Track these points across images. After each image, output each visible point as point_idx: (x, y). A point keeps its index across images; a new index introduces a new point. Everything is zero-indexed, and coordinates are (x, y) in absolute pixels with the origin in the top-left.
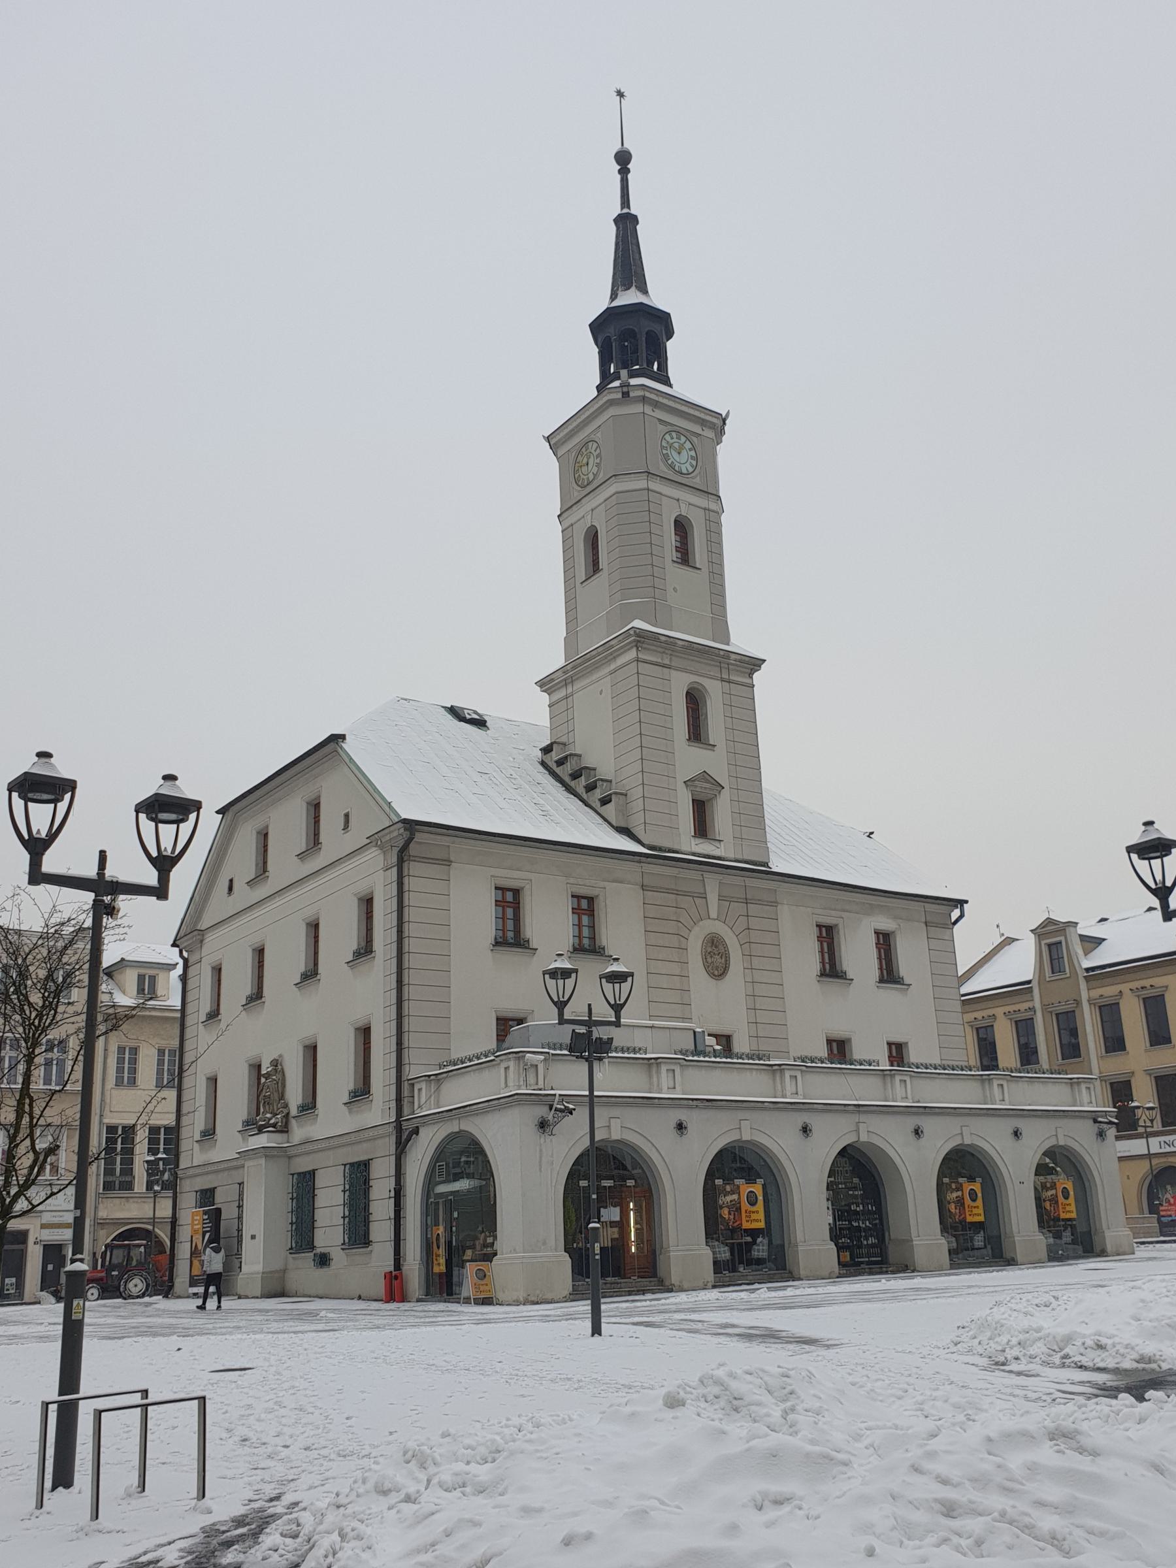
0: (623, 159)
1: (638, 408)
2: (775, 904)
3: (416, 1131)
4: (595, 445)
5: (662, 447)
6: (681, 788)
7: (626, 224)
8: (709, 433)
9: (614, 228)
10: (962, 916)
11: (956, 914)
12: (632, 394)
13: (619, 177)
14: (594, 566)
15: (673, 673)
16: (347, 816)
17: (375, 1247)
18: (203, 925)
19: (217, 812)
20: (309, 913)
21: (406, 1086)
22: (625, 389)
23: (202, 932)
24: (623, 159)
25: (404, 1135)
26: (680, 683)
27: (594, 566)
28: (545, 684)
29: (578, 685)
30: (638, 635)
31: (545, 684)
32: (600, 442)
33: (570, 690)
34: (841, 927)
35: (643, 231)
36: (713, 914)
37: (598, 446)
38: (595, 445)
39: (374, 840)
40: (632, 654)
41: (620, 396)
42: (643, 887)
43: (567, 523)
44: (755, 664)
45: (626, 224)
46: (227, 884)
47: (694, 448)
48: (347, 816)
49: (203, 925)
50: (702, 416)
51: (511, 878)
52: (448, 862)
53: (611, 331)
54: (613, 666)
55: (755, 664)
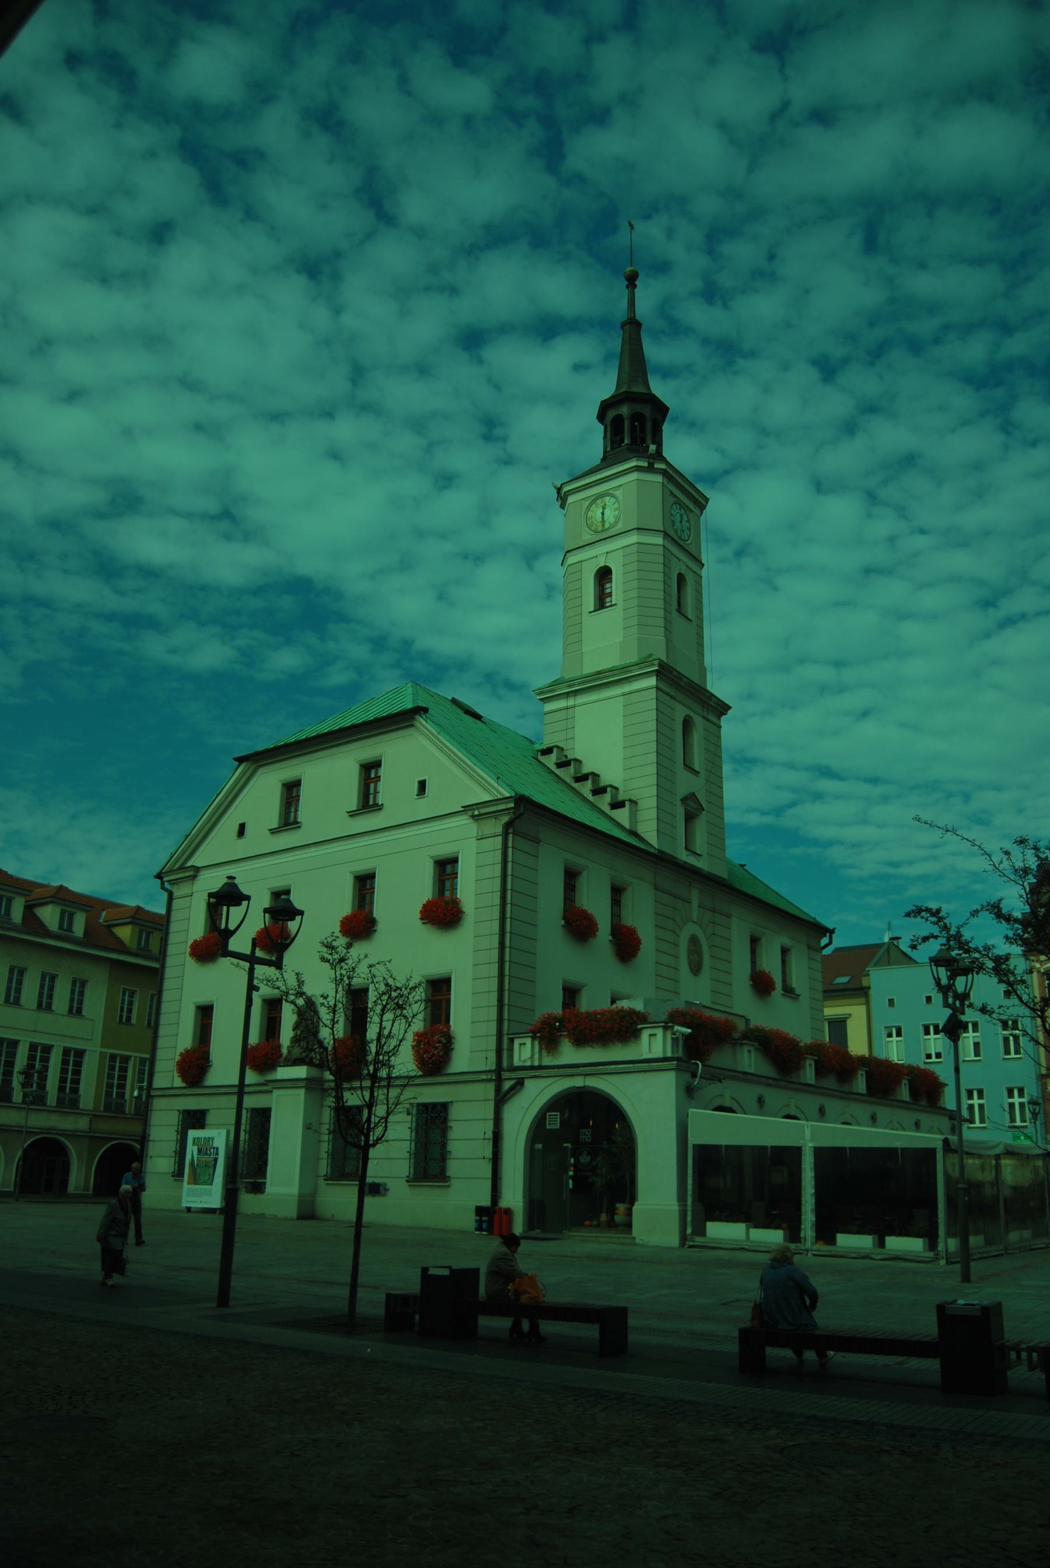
1: (659, 478)
2: (728, 916)
3: (520, 1083)
5: (672, 515)
6: (679, 804)
8: (697, 511)
10: (830, 943)
11: (824, 941)
12: (656, 466)
14: (602, 601)
16: (422, 785)
17: (453, 1182)
18: (196, 861)
19: (235, 759)
20: (363, 867)
21: (505, 1038)
23: (197, 869)
25: (504, 1082)
26: (680, 712)
27: (602, 601)
29: (581, 699)
30: (660, 665)
32: (621, 498)
34: (763, 940)
36: (695, 917)
37: (617, 501)
38: (613, 500)
39: (466, 808)
40: (652, 681)
41: (646, 464)
42: (656, 888)
44: (723, 708)
46: (237, 828)
47: (688, 521)
48: (422, 785)
49: (196, 861)
50: (697, 496)
51: (578, 861)
52: (537, 841)
54: (627, 688)
55: (723, 708)
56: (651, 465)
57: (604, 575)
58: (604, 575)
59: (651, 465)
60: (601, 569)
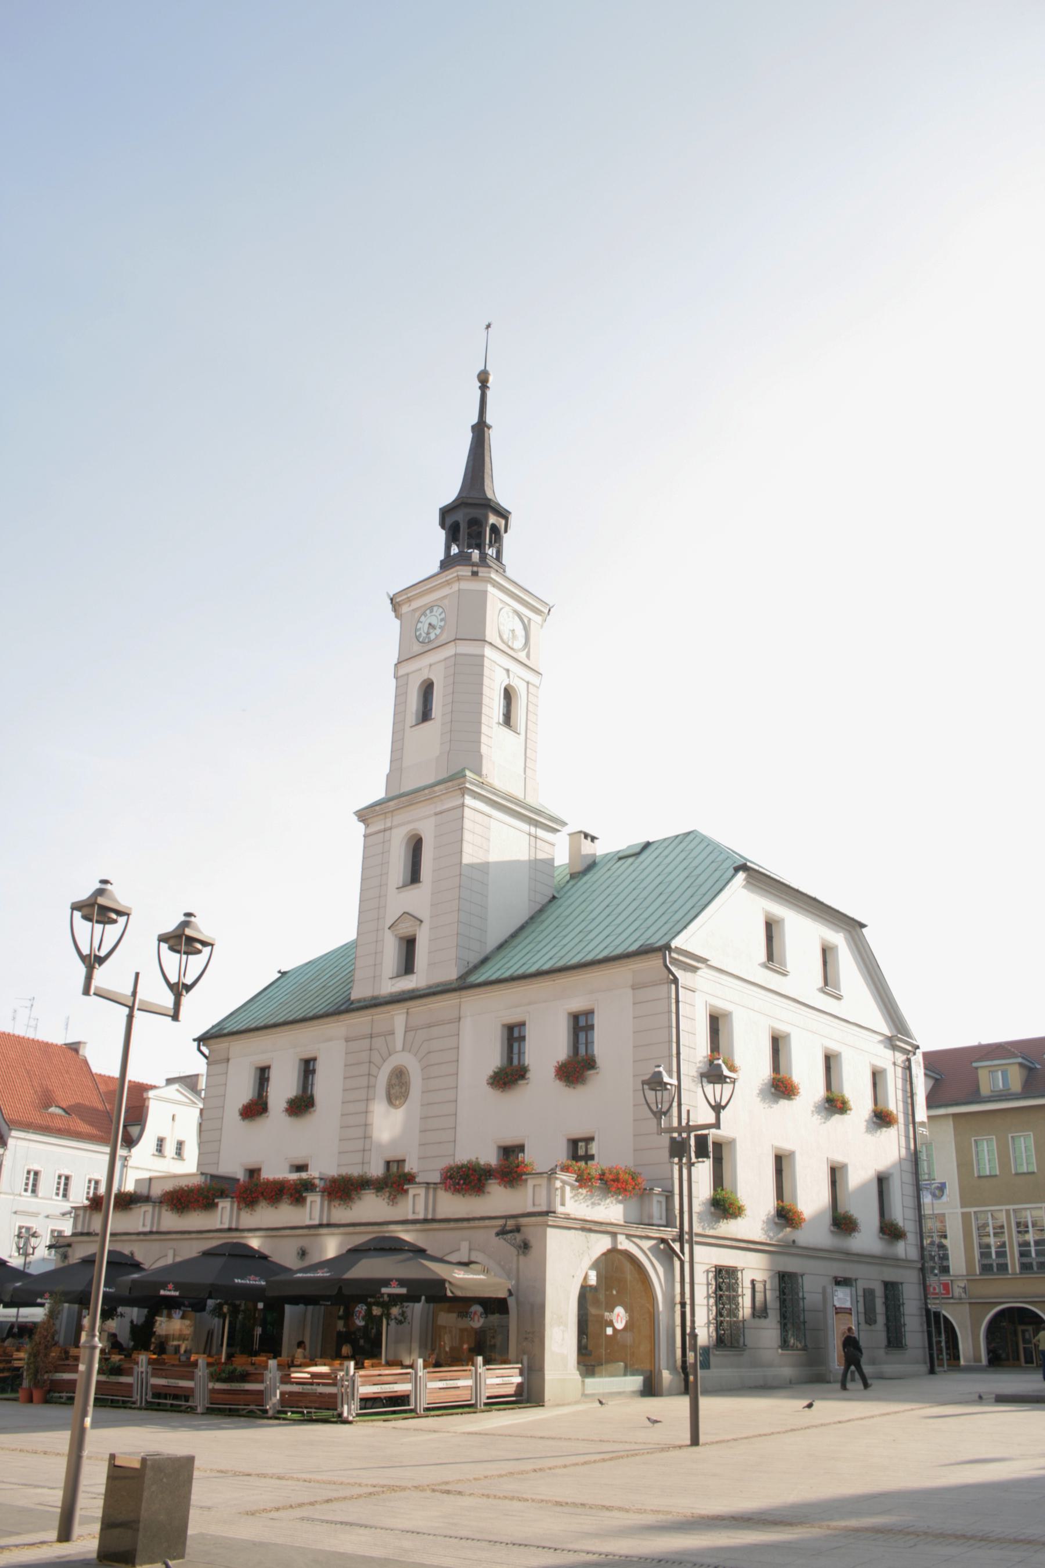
0: (483, 380)
4: (441, 610)
7: (480, 430)
9: (470, 435)
13: (479, 392)
14: (425, 715)
15: (493, 824)
22: (475, 569)
24: (483, 380)
27: (425, 715)
28: (364, 815)
31: (364, 815)
33: (389, 825)
35: (495, 438)
38: (441, 610)
43: (401, 672)
45: (480, 430)
53: (460, 516)
56: (475, 574)
57: (427, 690)
58: (427, 690)
59: (475, 574)
60: (425, 681)
